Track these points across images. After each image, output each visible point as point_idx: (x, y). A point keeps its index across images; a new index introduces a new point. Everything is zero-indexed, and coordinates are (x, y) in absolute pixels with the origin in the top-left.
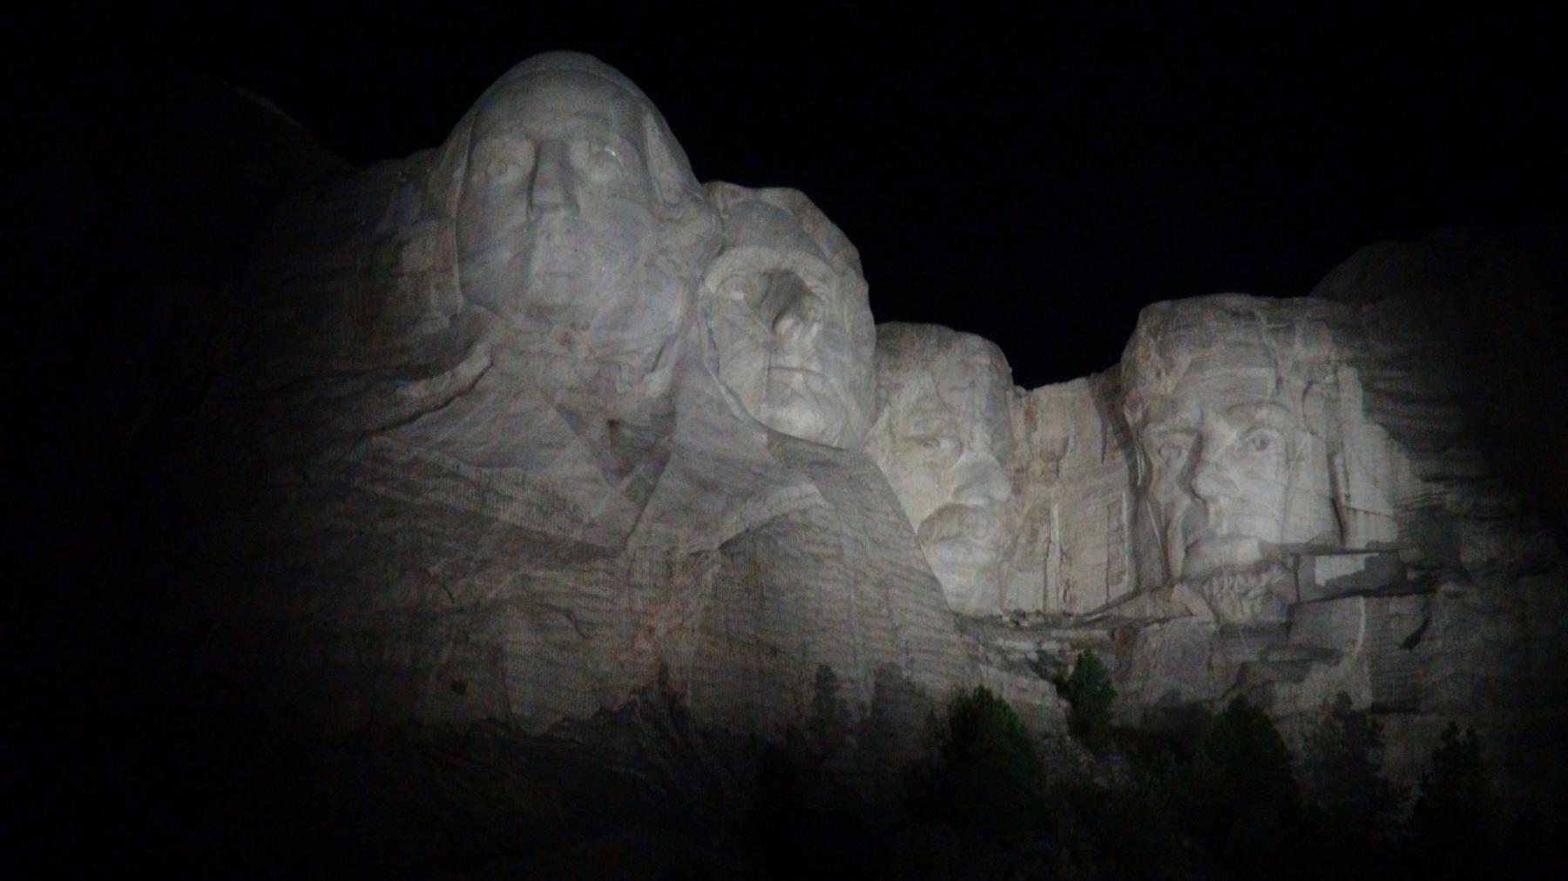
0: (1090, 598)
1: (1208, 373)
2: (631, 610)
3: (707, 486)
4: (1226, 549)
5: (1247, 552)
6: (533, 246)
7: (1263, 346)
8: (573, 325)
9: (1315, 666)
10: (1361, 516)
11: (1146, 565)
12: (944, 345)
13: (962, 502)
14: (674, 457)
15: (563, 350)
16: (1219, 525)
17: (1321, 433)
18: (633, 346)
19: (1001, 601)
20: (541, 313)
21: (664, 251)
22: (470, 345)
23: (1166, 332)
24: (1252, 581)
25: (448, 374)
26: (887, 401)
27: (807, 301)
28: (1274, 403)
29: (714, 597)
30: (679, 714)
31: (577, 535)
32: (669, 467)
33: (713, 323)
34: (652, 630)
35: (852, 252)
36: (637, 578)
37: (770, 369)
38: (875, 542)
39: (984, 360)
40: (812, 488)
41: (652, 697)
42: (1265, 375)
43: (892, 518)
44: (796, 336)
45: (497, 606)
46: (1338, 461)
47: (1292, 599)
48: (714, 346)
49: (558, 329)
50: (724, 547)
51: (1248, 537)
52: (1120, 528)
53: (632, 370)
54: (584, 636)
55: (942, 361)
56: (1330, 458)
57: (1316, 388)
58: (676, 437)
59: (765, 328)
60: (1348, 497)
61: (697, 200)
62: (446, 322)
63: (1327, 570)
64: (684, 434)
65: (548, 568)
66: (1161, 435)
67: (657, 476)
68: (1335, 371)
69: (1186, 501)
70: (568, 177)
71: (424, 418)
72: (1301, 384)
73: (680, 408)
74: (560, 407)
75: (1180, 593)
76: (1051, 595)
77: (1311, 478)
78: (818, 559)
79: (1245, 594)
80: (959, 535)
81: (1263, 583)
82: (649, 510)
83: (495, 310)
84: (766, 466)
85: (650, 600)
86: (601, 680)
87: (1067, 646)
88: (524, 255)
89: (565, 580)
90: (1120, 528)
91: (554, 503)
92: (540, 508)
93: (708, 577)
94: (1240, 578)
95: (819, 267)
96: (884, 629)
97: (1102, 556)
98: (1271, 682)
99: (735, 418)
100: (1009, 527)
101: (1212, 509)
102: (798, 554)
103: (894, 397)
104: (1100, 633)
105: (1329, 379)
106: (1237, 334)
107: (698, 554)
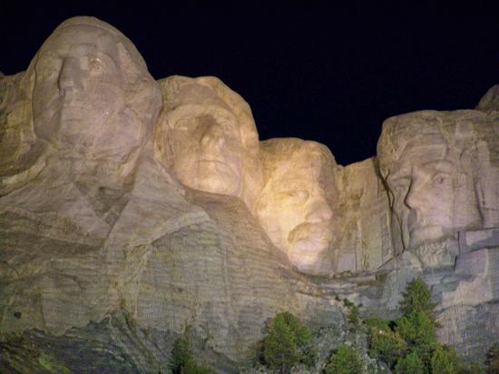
0: (375, 264)
1: (414, 149)
2: (106, 275)
3: (146, 215)
4: (426, 231)
5: (436, 233)
6: (62, 108)
7: (441, 134)
8: (85, 144)
9: (461, 283)
10: (490, 212)
11: (397, 246)
12: (297, 147)
13: (309, 221)
14: (131, 202)
15: (81, 156)
16: (422, 220)
17: (470, 174)
18: (114, 152)
19: (334, 267)
20: (69, 140)
21: (127, 106)
22: (37, 157)
23: (394, 131)
24: (438, 246)
25: (26, 172)
26: (270, 176)
27: (214, 128)
28: (445, 160)
29: (148, 266)
30: (130, 323)
31: (81, 241)
32: (127, 207)
33: (171, 143)
34: (116, 284)
35: (246, 106)
36: (108, 260)
37: (199, 161)
38: (237, 237)
39: (317, 153)
40: (203, 213)
41: (117, 315)
42: (441, 148)
43: (248, 226)
44: (211, 145)
45: (39, 277)
46: (478, 186)
47: (457, 253)
48: (172, 153)
49: (78, 146)
50: (153, 244)
51: (435, 226)
52: (386, 228)
53: (114, 163)
54: (82, 288)
55: (296, 155)
56: (475, 184)
57: (467, 152)
58: (133, 193)
59: (197, 143)
60: (484, 203)
61: (145, 81)
62: (28, 148)
63: (471, 239)
64: (137, 191)
65: (65, 257)
66: (395, 180)
67: (121, 211)
68: (476, 143)
69: (408, 211)
70: (79, 74)
71: (13, 193)
72: (460, 151)
73: (137, 179)
74: (77, 183)
75: (407, 254)
76: (359, 264)
77: (465, 195)
78: (205, 247)
79: (435, 253)
80: (307, 237)
81: (443, 246)
82: (117, 226)
83: (49, 140)
84: (181, 204)
85: (116, 270)
86: (91, 309)
87: (355, 285)
88: (59, 114)
89: (71, 264)
90: (386, 228)
91: (70, 227)
92: (63, 229)
93: (145, 257)
94: (433, 246)
95: (226, 112)
96: (243, 278)
97: (379, 242)
98: (441, 293)
99: (167, 182)
100: (335, 233)
101: (419, 214)
102: (194, 244)
103: (273, 173)
104: (372, 278)
105: (473, 147)
106: (427, 129)
107: (139, 247)
